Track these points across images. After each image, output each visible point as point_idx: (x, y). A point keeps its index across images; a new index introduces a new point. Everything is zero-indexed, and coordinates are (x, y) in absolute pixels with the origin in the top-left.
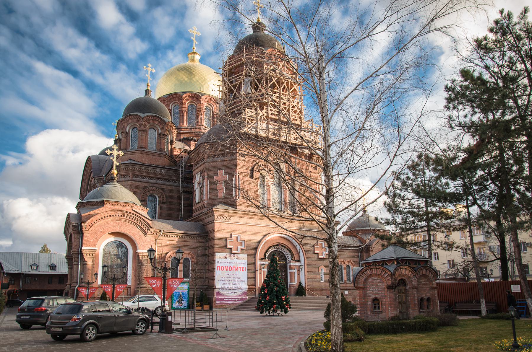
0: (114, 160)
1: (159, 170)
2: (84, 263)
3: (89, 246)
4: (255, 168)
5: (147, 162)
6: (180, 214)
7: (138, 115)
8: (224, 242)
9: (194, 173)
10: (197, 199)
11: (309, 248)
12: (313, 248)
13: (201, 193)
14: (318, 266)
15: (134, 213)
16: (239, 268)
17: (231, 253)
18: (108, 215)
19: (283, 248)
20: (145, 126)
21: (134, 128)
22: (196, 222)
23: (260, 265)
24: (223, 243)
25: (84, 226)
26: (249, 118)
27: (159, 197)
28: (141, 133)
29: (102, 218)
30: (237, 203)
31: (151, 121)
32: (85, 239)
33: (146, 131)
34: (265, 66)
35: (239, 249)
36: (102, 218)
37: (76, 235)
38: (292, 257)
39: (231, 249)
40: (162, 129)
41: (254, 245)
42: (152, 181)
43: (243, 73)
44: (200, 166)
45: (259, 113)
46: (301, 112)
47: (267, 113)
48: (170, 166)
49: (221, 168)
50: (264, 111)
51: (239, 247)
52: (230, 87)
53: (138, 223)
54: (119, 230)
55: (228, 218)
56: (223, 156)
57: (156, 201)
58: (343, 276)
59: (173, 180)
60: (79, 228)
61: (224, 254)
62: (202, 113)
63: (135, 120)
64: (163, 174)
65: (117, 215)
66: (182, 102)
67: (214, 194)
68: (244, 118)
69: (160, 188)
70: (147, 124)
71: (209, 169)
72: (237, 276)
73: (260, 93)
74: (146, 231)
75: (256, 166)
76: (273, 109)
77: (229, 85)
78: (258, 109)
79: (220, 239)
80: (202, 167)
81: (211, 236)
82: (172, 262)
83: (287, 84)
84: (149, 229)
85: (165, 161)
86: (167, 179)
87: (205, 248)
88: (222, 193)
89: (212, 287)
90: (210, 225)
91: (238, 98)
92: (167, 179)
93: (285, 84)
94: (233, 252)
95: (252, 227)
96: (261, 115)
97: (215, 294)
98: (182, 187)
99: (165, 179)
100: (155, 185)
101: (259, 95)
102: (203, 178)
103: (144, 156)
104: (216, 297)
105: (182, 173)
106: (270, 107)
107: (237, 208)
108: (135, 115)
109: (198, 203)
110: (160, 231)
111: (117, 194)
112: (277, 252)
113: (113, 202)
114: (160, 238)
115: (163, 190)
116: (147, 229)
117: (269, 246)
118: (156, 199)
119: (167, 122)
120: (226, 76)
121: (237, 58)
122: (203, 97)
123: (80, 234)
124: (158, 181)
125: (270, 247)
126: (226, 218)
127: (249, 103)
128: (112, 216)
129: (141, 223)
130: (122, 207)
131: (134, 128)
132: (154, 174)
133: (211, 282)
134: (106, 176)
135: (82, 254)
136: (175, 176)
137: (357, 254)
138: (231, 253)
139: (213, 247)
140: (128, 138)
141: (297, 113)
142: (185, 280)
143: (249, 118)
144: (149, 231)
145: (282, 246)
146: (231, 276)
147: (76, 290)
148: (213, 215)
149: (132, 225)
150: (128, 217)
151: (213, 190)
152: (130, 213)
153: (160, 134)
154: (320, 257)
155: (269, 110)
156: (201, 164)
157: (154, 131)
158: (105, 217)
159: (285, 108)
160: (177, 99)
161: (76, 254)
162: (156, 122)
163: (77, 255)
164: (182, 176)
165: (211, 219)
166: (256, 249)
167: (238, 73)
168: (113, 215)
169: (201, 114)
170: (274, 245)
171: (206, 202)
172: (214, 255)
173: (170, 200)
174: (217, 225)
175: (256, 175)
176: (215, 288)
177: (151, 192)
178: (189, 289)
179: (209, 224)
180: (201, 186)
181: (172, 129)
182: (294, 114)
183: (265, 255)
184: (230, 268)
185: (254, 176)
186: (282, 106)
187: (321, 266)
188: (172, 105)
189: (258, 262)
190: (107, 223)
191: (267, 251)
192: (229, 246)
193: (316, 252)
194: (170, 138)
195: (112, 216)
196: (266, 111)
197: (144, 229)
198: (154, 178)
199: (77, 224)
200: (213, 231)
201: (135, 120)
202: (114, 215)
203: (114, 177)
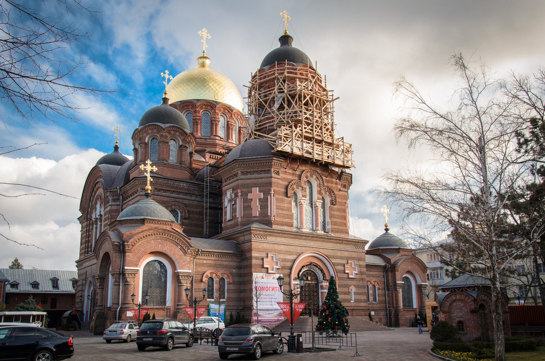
0: (148, 175)
1: (182, 184)
2: (126, 283)
3: (132, 266)
4: (289, 186)
5: (168, 175)
6: (205, 230)
7: (159, 126)
8: (261, 261)
9: (224, 189)
10: (228, 217)
11: (341, 268)
12: (343, 267)
13: (234, 210)
14: (348, 286)
15: (174, 231)
16: (275, 289)
17: (267, 272)
18: (150, 234)
19: (315, 268)
20: (166, 137)
21: (153, 139)
22: (227, 240)
23: (294, 284)
24: (259, 262)
25: (128, 245)
26: (285, 136)
27: (181, 213)
28: (161, 144)
29: (144, 237)
30: (272, 222)
31: (172, 132)
32: (127, 258)
33: (168, 143)
34: (298, 83)
35: (274, 269)
36: (144, 237)
37: (117, 254)
38: (324, 277)
39: (267, 268)
40: (183, 140)
41: (289, 264)
42: (174, 195)
43: (276, 87)
44: (231, 183)
45: (294, 131)
46: (332, 130)
47: (301, 130)
48: (191, 179)
49: (255, 185)
50: (298, 129)
51: (275, 267)
52: (261, 102)
53: (178, 242)
54: (159, 249)
55: (265, 237)
56: (258, 174)
57: (178, 217)
58: (370, 296)
59: (195, 195)
60: (121, 247)
61: (261, 274)
62: (217, 123)
63: (155, 131)
64: (185, 189)
65: (158, 234)
66: (196, 111)
67: (248, 213)
68: (279, 135)
69: (182, 203)
70: (168, 135)
71: (243, 186)
72: (273, 297)
73: (294, 110)
74: (186, 250)
75: (290, 184)
76: (306, 126)
77: (259, 99)
78: (293, 127)
79: (257, 258)
80: (234, 184)
81: (248, 255)
82: (208, 282)
83: (320, 101)
84: (189, 249)
85: (185, 175)
86: (189, 194)
87: (240, 268)
88: (256, 212)
89: (250, 308)
90: (245, 244)
91: (270, 113)
92: (189, 194)
93: (317, 102)
94: (270, 271)
95: (286, 246)
96: (296, 132)
97: (253, 315)
98: (206, 202)
99: (187, 193)
100: (177, 200)
101: (292, 112)
102: (236, 196)
103: (166, 168)
104: (255, 318)
105: (207, 188)
106: (304, 125)
107: (273, 226)
108: (155, 125)
109: (229, 221)
110: (198, 251)
111: (155, 211)
112: (309, 272)
113: (153, 220)
114: (198, 257)
115: (185, 205)
116: (187, 248)
117: (302, 265)
118: (178, 214)
119: (188, 133)
120: (256, 90)
121: (268, 73)
122: (218, 106)
123: (121, 253)
124: (180, 196)
125: (303, 267)
126: (262, 237)
127: (283, 119)
128: (153, 234)
129: (181, 242)
130: (161, 226)
131: (153, 139)
132: (177, 188)
133: (247, 303)
134: (121, 188)
135: (124, 274)
136: (197, 190)
137: (382, 274)
138: (267, 272)
139: (250, 266)
140: (147, 149)
141: (329, 131)
142: (222, 300)
143: (285, 136)
144: (189, 251)
145: (314, 265)
146: (268, 297)
147: (118, 311)
148: (251, 234)
149: (173, 244)
150: (169, 236)
151: (247, 207)
152: (171, 232)
153: (181, 146)
154: (350, 276)
155: (303, 128)
156: (232, 180)
157: (175, 143)
158: (146, 236)
159: (318, 126)
160: (190, 106)
161: (117, 274)
162: (178, 134)
163: (119, 275)
164: (206, 191)
165: (247, 238)
166: (291, 268)
167: (269, 88)
168: (154, 234)
169: (216, 124)
170: (307, 264)
171: (240, 220)
172: (251, 275)
173: (192, 216)
174: (254, 245)
175: (290, 192)
176: (253, 309)
177: (173, 207)
178: (226, 310)
179: (244, 243)
180: (233, 203)
181: (191, 141)
182: (326, 132)
183: (298, 274)
184: (267, 288)
185: (289, 195)
186: (315, 124)
187: (351, 286)
188: (185, 112)
189: (293, 282)
190: (148, 242)
191: (300, 271)
192: (265, 266)
193: (347, 272)
194: (189, 150)
195: (153, 234)
196: (300, 128)
197: (184, 248)
198: (176, 192)
199: (119, 243)
200: (250, 250)
201: (155, 131)
202: (156, 234)
203: (148, 193)
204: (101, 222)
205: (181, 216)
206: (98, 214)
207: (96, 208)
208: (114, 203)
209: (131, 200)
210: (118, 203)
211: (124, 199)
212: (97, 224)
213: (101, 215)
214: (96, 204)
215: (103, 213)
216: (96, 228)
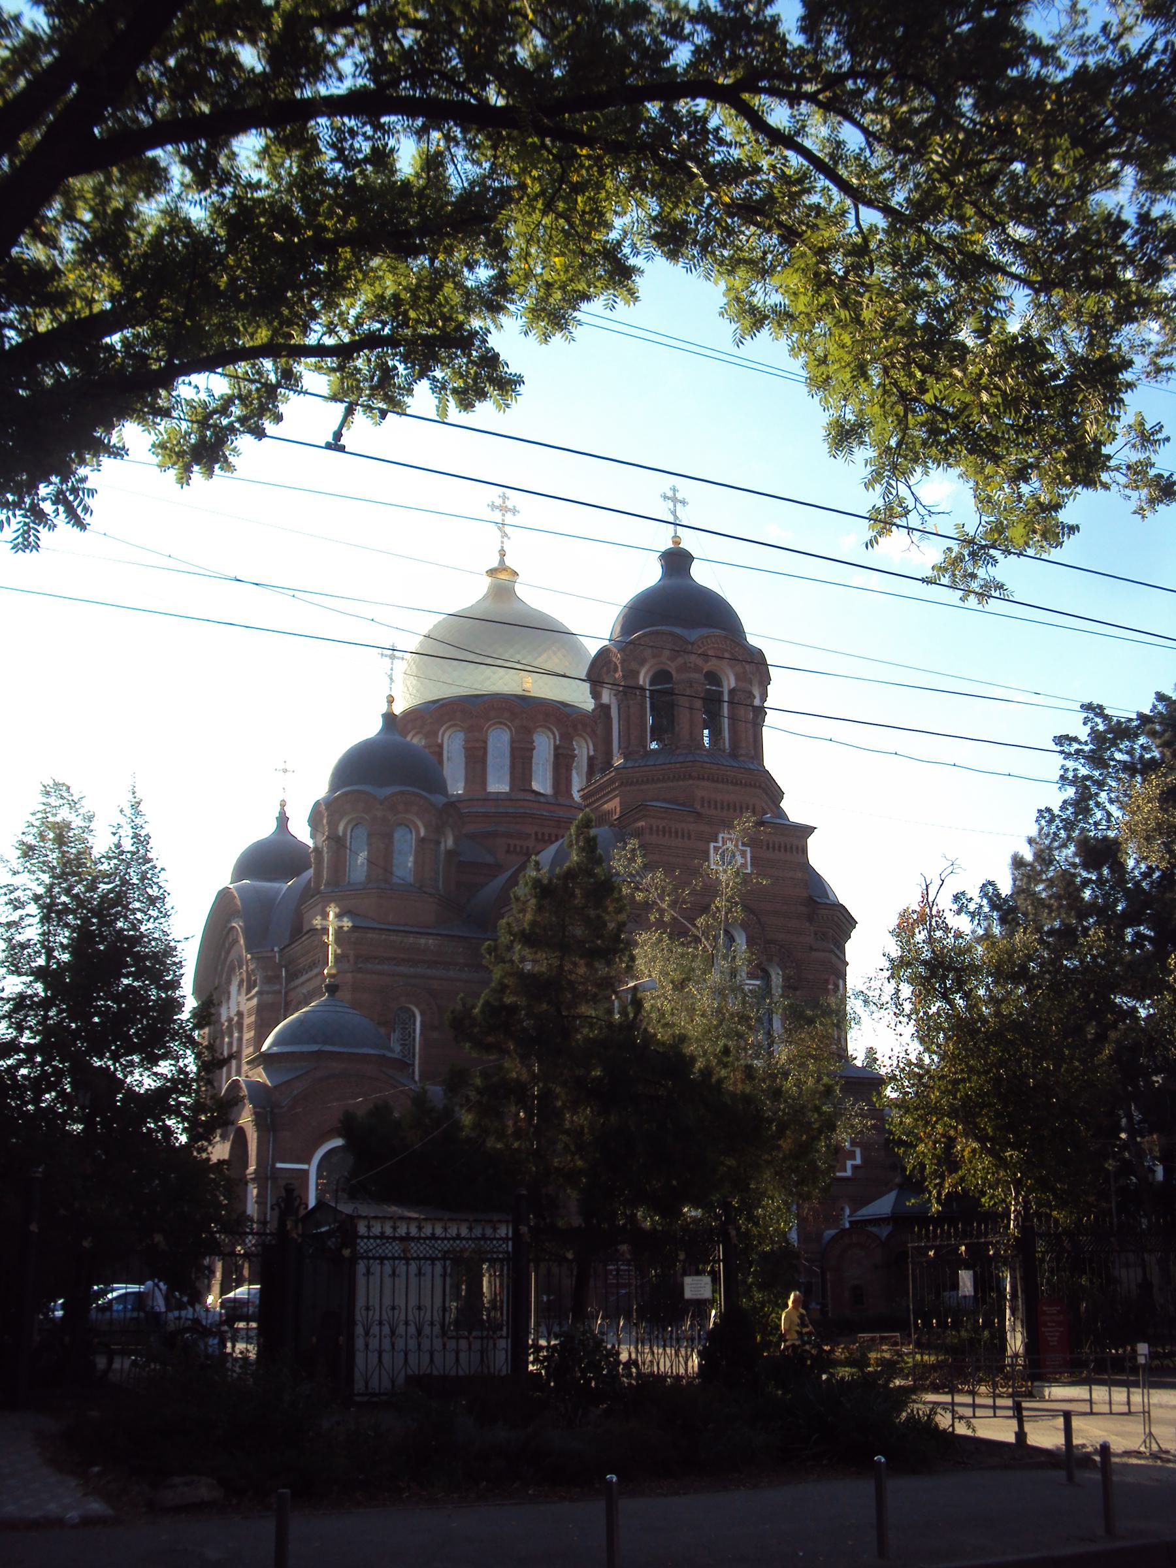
1: (423, 941)
27: (422, 1014)
42: (402, 969)
118: (414, 1016)
154: (839, 1174)
205: (422, 1023)
207: (229, 993)
208: (267, 988)
209: (303, 984)
210: (277, 987)
211: (292, 976)
212: (231, 1036)
213: (240, 1014)
214: (229, 982)
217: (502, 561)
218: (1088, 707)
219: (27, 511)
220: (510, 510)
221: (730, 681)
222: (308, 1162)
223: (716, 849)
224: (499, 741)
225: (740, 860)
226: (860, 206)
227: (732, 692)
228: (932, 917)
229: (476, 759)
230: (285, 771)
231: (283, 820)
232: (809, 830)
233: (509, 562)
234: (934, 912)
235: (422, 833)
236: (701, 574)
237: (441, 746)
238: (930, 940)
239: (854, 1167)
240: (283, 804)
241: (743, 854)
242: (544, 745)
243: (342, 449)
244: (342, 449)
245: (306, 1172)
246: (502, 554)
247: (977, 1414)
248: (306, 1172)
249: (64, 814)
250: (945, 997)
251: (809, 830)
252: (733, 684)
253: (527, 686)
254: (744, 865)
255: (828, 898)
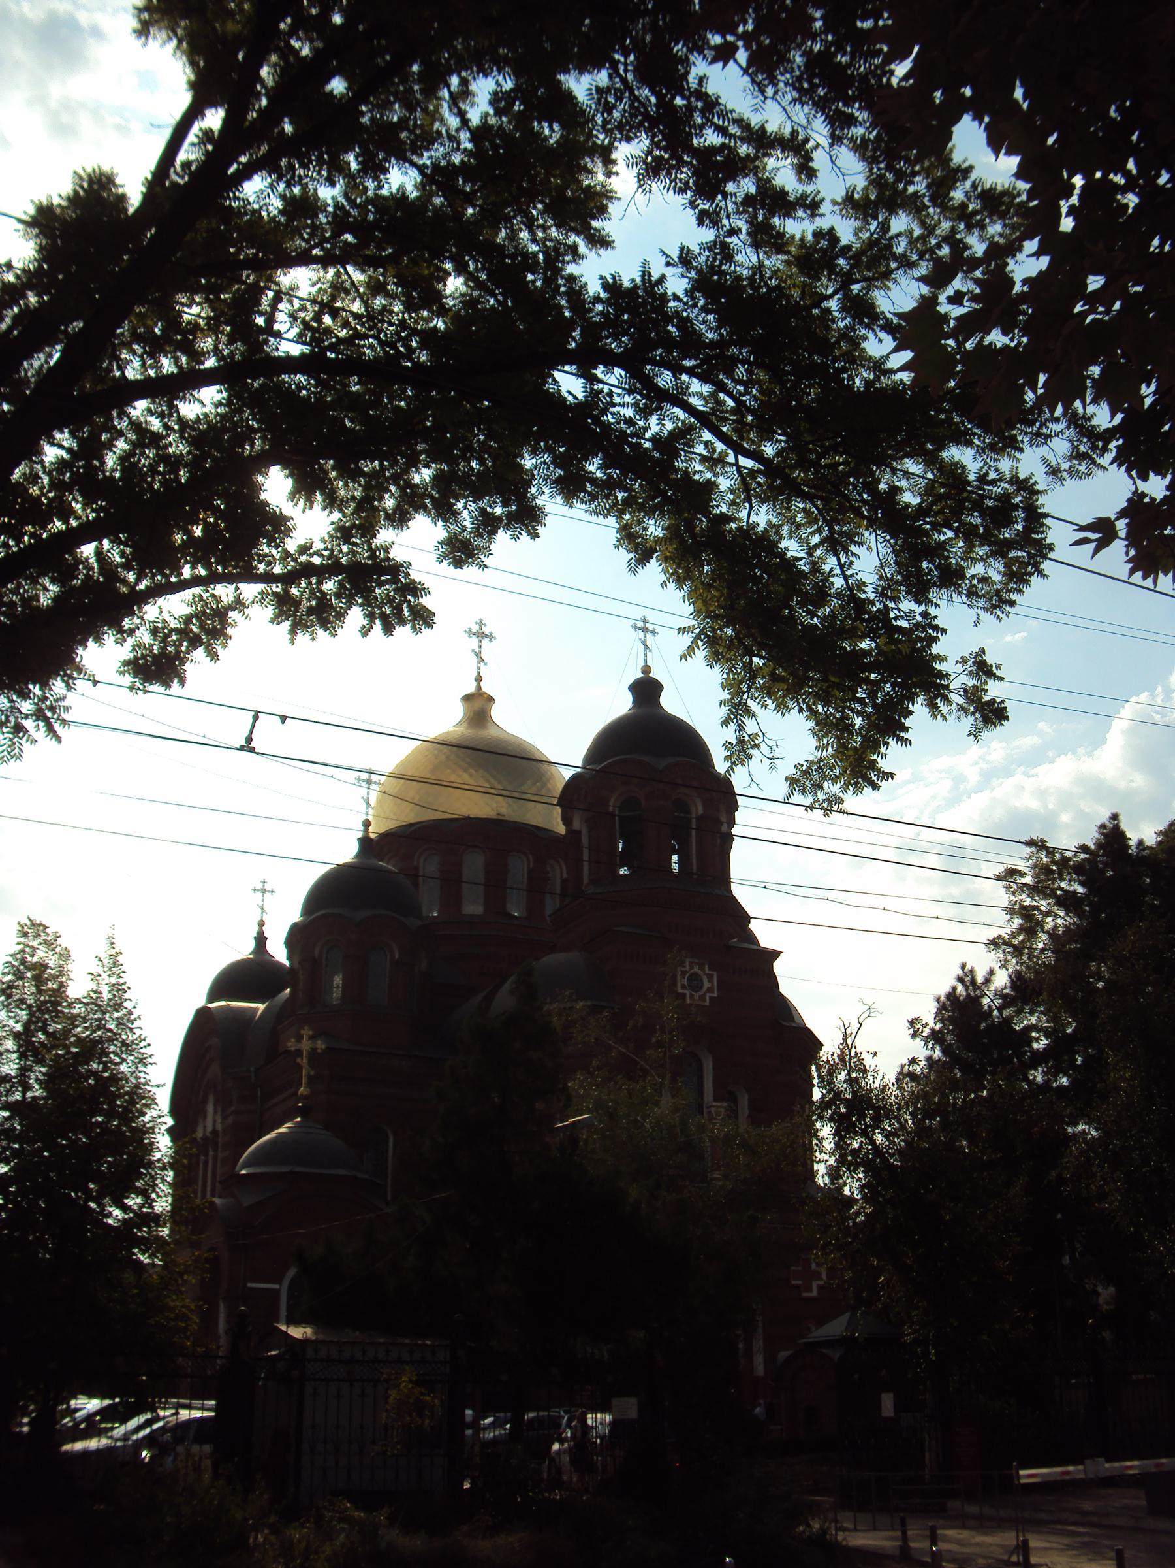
154: (805, 1294)
204: (215, 1150)
206: (210, 1128)
212: (206, 1155)
215: (219, 1127)
216: (206, 1163)
217: (479, 687)
218: (1030, 843)
219: (11, 728)
220: (487, 636)
221: (698, 808)
222: (279, 1282)
223: (684, 973)
224: (474, 865)
225: (706, 984)
226: (740, 457)
227: (699, 819)
228: (851, 1057)
229: (451, 883)
230: (264, 891)
231: (261, 940)
232: (775, 954)
233: (485, 687)
234: (853, 1054)
235: (397, 956)
236: (670, 703)
237: (417, 869)
238: (850, 1081)
239: (820, 1288)
240: (262, 924)
241: (710, 977)
242: (519, 869)
243: (252, 750)
244: (252, 750)
245: (277, 1292)
246: (479, 679)
247: (858, 1528)
248: (277, 1292)
249: (41, 954)
250: (864, 1133)
251: (775, 954)
252: (701, 811)
253: (504, 811)
254: (710, 990)
255: (793, 1020)
